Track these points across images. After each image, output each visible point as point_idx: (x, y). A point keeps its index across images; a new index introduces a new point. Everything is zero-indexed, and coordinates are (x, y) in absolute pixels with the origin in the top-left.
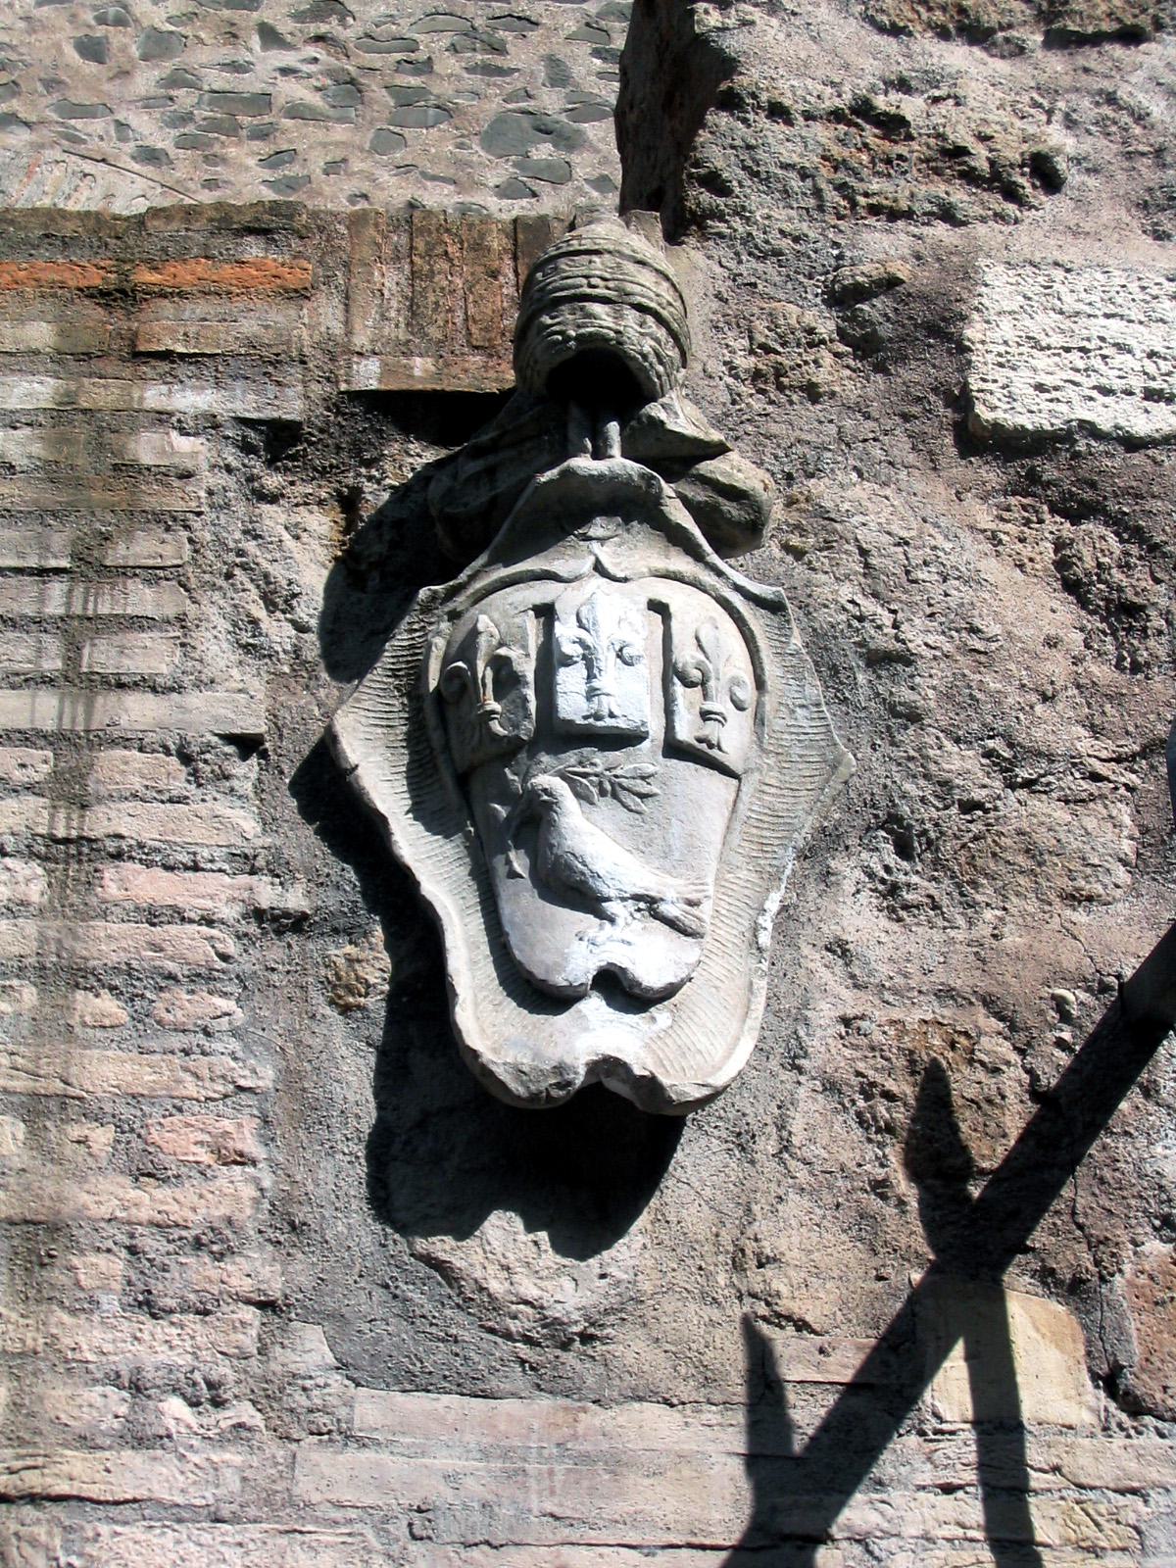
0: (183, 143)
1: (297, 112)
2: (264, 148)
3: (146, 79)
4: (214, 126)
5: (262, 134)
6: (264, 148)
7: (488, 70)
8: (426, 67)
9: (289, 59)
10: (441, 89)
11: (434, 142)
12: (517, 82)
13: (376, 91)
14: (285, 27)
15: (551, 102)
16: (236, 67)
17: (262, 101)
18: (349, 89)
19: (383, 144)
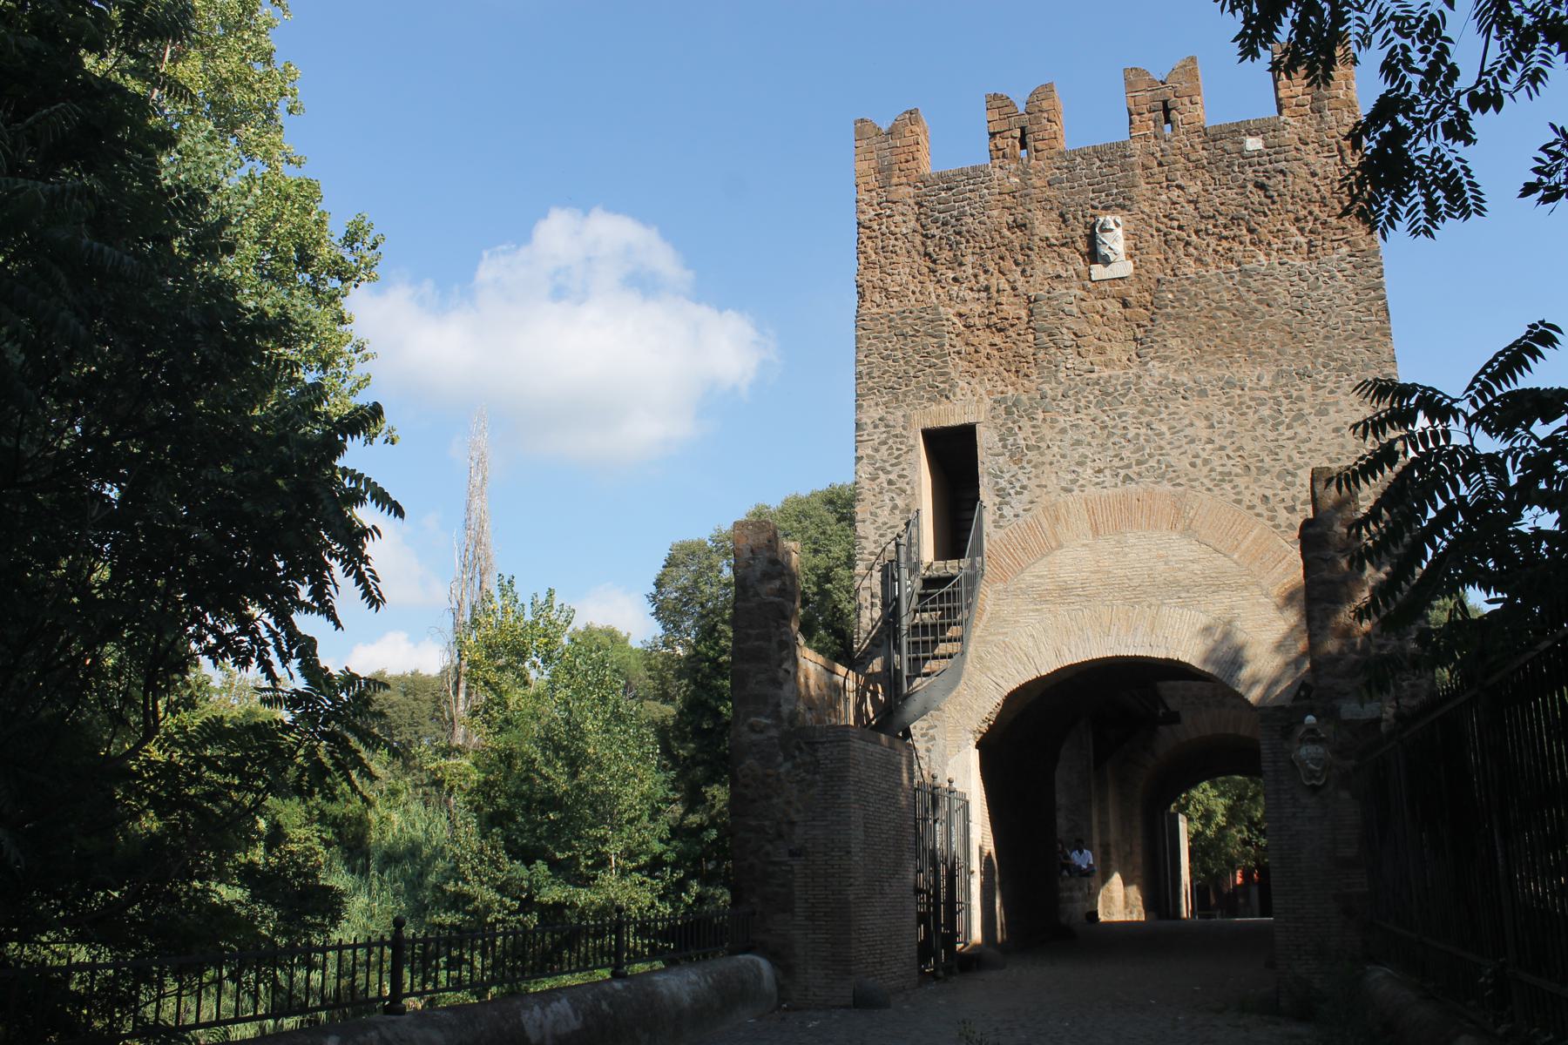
0: (1215, 486)
1: (1236, 475)
2: (1232, 485)
3: (1205, 470)
4: (1221, 480)
5: (1231, 481)
6: (1232, 485)
8: (1262, 461)
9: (1232, 462)
10: (1266, 466)
11: (1266, 479)
12: (1282, 462)
13: (1252, 468)
14: (1231, 454)
15: (1290, 466)
16: (1223, 465)
17: (1230, 474)
19: (1256, 480)
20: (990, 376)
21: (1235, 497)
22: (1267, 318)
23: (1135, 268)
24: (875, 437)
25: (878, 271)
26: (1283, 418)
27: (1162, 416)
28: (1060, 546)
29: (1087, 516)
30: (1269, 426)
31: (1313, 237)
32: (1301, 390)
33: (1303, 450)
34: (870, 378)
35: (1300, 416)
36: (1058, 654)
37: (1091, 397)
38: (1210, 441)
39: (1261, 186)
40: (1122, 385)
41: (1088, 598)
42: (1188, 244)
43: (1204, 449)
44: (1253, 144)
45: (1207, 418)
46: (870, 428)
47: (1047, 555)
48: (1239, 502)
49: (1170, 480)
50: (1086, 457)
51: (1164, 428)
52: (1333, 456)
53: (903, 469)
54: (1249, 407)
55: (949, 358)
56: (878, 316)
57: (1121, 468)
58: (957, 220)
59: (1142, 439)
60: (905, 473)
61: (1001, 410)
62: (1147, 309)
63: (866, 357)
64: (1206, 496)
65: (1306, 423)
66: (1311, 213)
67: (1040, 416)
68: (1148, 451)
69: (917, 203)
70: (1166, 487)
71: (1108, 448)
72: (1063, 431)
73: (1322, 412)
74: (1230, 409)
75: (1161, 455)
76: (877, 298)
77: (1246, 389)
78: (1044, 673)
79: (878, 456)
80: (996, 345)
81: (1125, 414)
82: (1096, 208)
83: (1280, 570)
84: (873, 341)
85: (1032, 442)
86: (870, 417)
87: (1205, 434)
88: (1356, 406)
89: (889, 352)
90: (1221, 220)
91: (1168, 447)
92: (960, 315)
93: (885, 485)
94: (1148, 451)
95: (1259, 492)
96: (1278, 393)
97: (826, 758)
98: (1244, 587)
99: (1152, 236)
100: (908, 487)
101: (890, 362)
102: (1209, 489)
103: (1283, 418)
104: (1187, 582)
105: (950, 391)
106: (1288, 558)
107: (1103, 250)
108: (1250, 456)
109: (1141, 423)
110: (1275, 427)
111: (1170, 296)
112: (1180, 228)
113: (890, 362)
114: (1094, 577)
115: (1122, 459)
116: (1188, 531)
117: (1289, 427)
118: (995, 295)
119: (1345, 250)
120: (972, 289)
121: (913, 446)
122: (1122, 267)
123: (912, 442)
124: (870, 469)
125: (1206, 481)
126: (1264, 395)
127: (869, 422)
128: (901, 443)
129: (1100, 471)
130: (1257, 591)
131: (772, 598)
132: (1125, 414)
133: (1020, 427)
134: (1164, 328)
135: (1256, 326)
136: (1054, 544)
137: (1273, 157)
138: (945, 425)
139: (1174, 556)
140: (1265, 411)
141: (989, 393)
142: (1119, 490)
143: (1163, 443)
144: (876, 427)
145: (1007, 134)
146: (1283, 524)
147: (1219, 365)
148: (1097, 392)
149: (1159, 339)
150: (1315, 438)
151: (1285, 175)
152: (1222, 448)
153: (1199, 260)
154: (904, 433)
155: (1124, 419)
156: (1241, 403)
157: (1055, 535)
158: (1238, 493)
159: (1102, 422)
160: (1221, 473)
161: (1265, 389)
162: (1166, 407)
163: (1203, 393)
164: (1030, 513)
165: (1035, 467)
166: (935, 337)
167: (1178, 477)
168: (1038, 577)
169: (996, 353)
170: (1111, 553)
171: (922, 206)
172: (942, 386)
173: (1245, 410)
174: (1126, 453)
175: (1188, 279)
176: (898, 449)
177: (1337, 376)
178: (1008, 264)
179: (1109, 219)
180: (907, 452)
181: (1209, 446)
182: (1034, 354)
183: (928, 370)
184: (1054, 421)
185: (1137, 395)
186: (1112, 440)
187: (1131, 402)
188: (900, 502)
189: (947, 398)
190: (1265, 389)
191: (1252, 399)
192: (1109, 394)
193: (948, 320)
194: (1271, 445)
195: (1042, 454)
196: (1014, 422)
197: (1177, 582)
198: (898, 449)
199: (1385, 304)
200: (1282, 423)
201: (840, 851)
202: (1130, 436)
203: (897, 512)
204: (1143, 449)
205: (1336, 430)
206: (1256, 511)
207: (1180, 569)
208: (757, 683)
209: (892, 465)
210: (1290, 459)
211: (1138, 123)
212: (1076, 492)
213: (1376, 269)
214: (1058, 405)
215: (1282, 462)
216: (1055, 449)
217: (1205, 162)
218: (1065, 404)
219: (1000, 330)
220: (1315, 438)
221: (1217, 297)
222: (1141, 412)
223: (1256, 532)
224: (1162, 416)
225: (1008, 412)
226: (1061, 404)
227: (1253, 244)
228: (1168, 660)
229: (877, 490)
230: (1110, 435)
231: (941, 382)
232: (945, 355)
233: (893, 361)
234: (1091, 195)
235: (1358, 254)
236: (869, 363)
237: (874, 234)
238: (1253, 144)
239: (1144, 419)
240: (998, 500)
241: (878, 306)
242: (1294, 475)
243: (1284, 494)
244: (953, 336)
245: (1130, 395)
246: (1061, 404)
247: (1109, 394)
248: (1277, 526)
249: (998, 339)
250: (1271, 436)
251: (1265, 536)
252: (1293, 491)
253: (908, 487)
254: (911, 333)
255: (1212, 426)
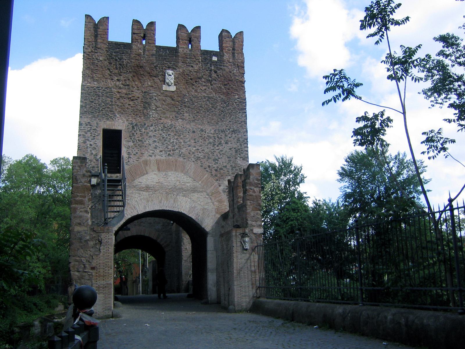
0: (195, 160)
1: (202, 158)
3: (193, 156)
7: (213, 155)
11: (210, 160)
14: (201, 152)
15: (217, 158)
17: (200, 157)
18: (205, 157)
20: (128, 115)
21: (201, 165)
22: (214, 112)
23: (176, 89)
24: (86, 128)
25: (90, 71)
26: (216, 143)
27: (181, 137)
28: (147, 173)
29: (156, 165)
30: (212, 145)
31: (228, 91)
32: (222, 136)
33: (221, 153)
34: (85, 108)
35: (220, 143)
36: (145, 207)
37: (160, 128)
38: (195, 147)
39: (216, 72)
40: (170, 125)
41: (156, 191)
42: (193, 85)
43: (193, 149)
44: (215, 59)
45: (195, 140)
46: (84, 126)
47: (143, 176)
48: (202, 166)
49: (183, 157)
50: (157, 146)
51: (181, 141)
52: (229, 156)
53: (96, 141)
54: (207, 138)
55: (114, 106)
56: (90, 87)
57: (168, 151)
58: (120, 60)
59: (175, 143)
60: (96, 142)
61: (131, 126)
62: (179, 102)
63: (85, 100)
64: (193, 163)
65: (222, 146)
66: (228, 83)
67: (143, 130)
68: (176, 147)
69: (106, 51)
70: (181, 159)
71: (164, 145)
72: (150, 137)
73: (226, 143)
74: (202, 138)
75: (180, 149)
76: (89, 80)
77: (206, 133)
78: (140, 213)
79: (86, 135)
80: (130, 105)
81: (170, 135)
82: (166, 67)
83: (212, 188)
84: (87, 95)
85: (140, 139)
86: (84, 121)
87: (193, 144)
88: (236, 143)
89: (93, 100)
90: (203, 80)
91: (182, 147)
92: (118, 92)
93: (89, 146)
94: (176, 147)
95: (208, 164)
96: (215, 135)
97: (104, 238)
98: (202, 192)
99: (183, 80)
100: (97, 147)
101: (93, 104)
102: (193, 161)
103: (216, 143)
104: (185, 189)
105: (114, 117)
106: (214, 185)
107: (167, 81)
108: (206, 153)
109: (175, 138)
110: (214, 146)
111: (186, 100)
112: (191, 79)
113: (93, 104)
114: (157, 184)
115: (168, 148)
116: (186, 173)
117: (218, 146)
118: (131, 88)
119: (237, 97)
120: (123, 84)
121: (99, 134)
122: (173, 88)
123: (99, 132)
124: (83, 139)
125: (193, 159)
126: (212, 135)
127: (84, 123)
128: (95, 132)
129: (161, 151)
130: (205, 194)
131: (86, 184)
132: (170, 135)
133: (136, 133)
134: (184, 110)
135: (211, 114)
136: (145, 172)
137: (220, 64)
138: (112, 128)
139: (182, 180)
140: (211, 140)
141: (127, 120)
142: (167, 158)
143: (181, 145)
144: (87, 125)
145: (139, 35)
146: (214, 174)
147: (199, 124)
148: (162, 126)
149: (182, 113)
150: (224, 151)
151: (223, 70)
152: (198, 149)
153: (196, 91)
154: (97, 129)
155: (170, 136)
156: (205, 137)
157: (146, 169)
158: (202, 164)
159: (163, 136)
160: (197, 157)
161: (211, 133)
162: (183, 134)
163: (194, 132)
164: (138, 162)
165: (141, 147)
166: (110, 98)
167: (185, 156)
168: (139, 182)
169: (130, 107)
170: (163, 177)
171: (108, 52)
172: (111, 115)
173: (205, 139)
174: (169, 147)
175: (192, 96)
176: (94, 134)
177: (232, 133)
178: (136, 79)
179: (170, 72)
180: (97, 135)
181: (194, 148)
182: (143, 110)
183: (106, 109)
184: (147, 133)
185: (174, 129)
186: (166, 142)
187: (172, 131)
188: (93, 152)
189: (113, 120)
190: (211, 133)
191: (208, 136)
192: (166, 127)
193: (115, 93)
194: (212, 151)
195: (143, 143)
196: (134, 131)
197: (182, 188)
198: (94, 134)
199: (246, 114)
200: (215, 145)
201: (108, 268)
202: (171, 141)
203: (93, 156)
204: (175, 146)
205: (230, 149)
206: (207, 169)
207: (183, 185)
208: (80, 212)
209: (92, 139)
210: (217, 156)
211: (181, 43)
212: (153, 157)
213: (245, 104)
214: (149, 128)
215: (214, 156)
216: (147, 142)
217: (200, 61)
218: (151, 128)
219: (132, 100)
220: (224, 151)
221: (200, 103)
222: (175, 135)
223: (206, 176)
224: (181, 137)
225: (133, 127)
226: (150, 128)
227: (212, 89)
228: (178, 212)
229: (86, 147)
230: (165, 140)
231: (111, 114)
232: (113, 105)
233: (95, 104)
234: (165, 62)
235: (240, 98)
236: (85, 103)
237: (90, 58)
238: (215, 59)
239: (176, 137)
240: (127, 156)
241: (90, 83)
242: (218, 161)
243: (214, 166)
244: (116, 99)
245: (172, 129)
246: (150, 128)
247: (166, 127)
248: (212, 175)
249: (131, 103)
250: (212, 148)
251: (209, 177)
252: (217, 165)
253: (97, 147)
254: (101, 95)
255: (196, 142)
